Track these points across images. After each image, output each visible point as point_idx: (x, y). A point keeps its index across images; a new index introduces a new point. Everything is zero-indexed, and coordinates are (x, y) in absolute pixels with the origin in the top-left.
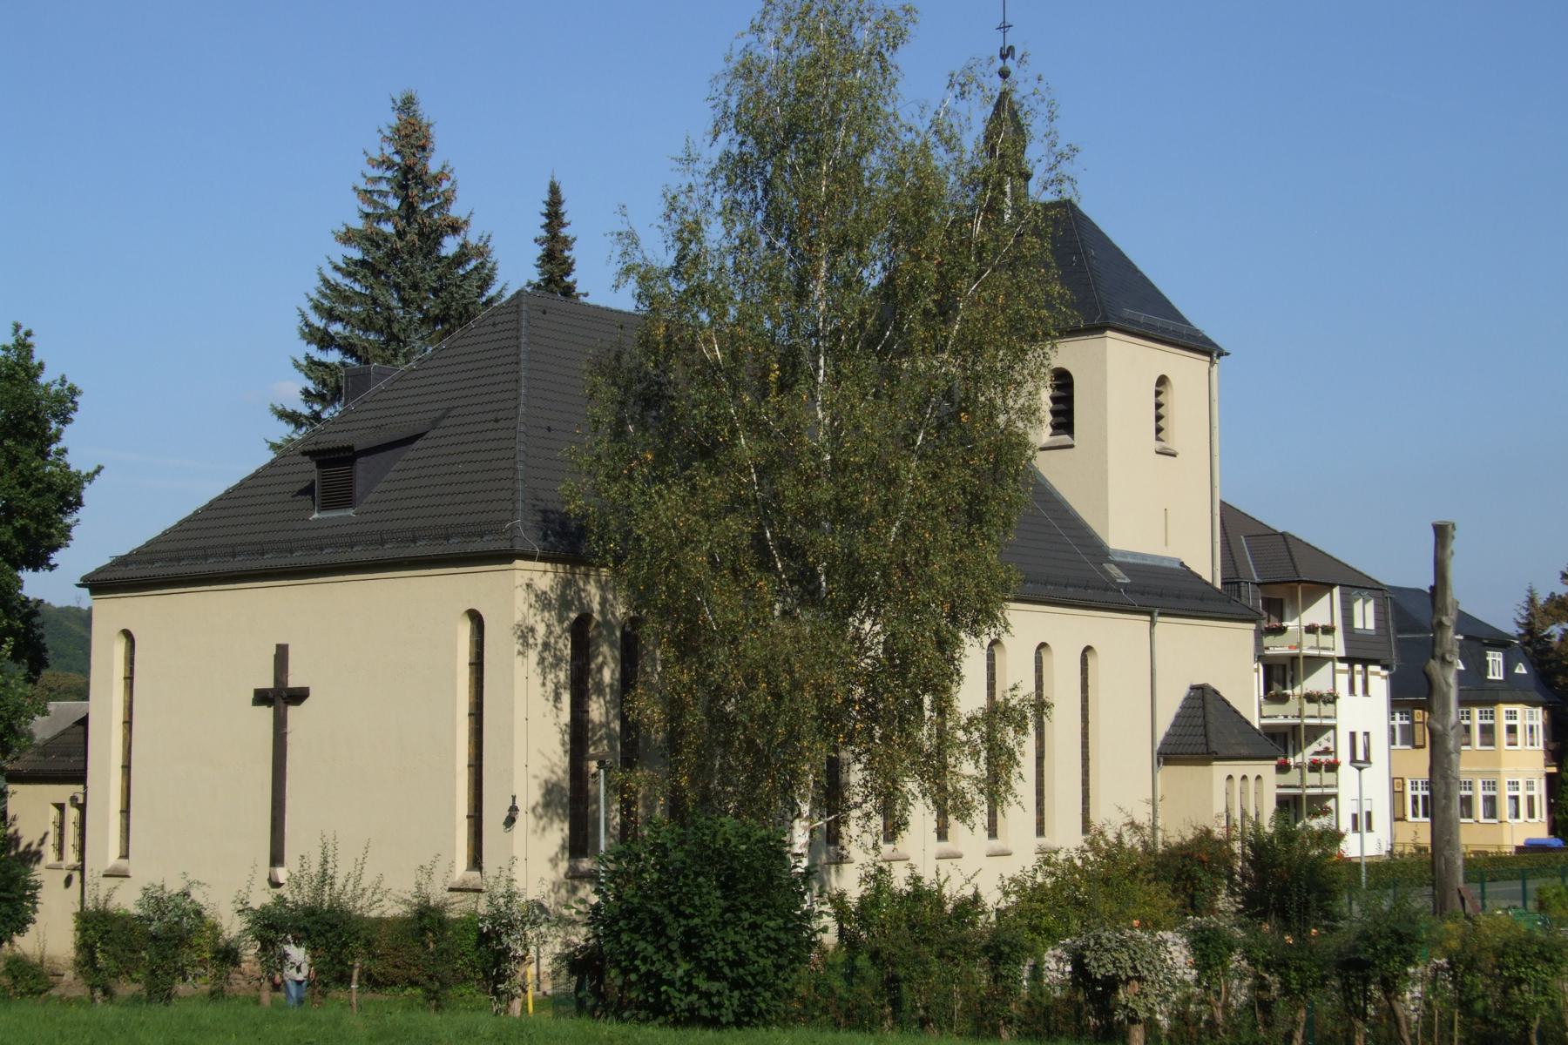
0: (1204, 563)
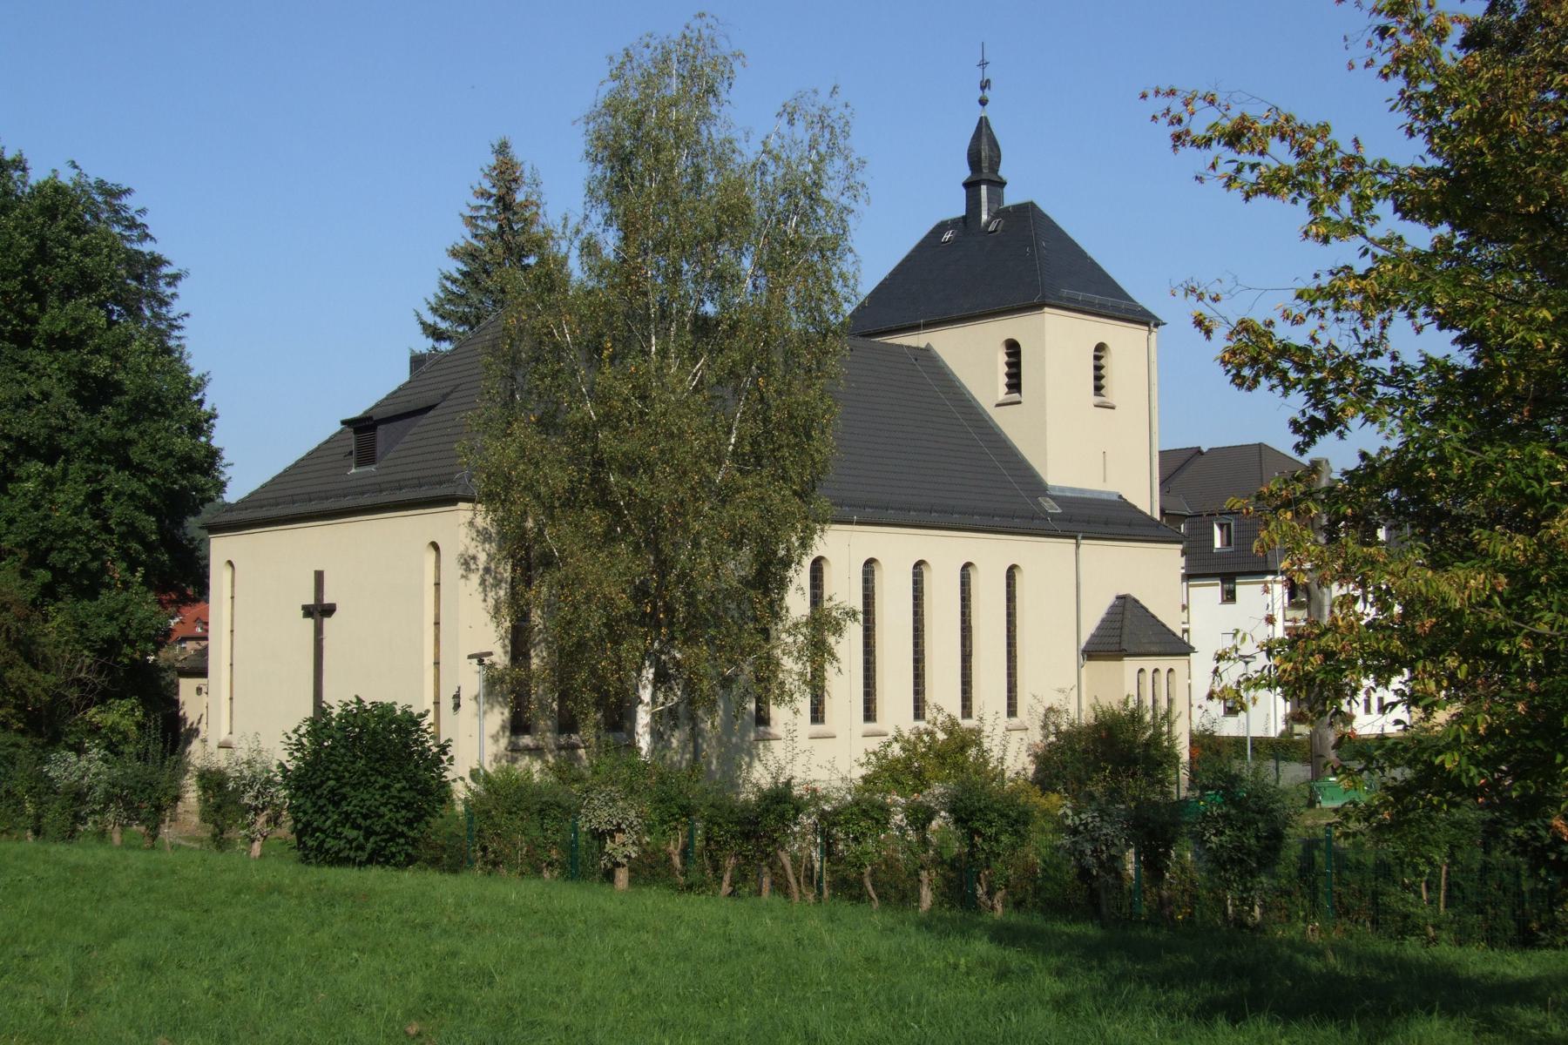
0: (1144, 496)
